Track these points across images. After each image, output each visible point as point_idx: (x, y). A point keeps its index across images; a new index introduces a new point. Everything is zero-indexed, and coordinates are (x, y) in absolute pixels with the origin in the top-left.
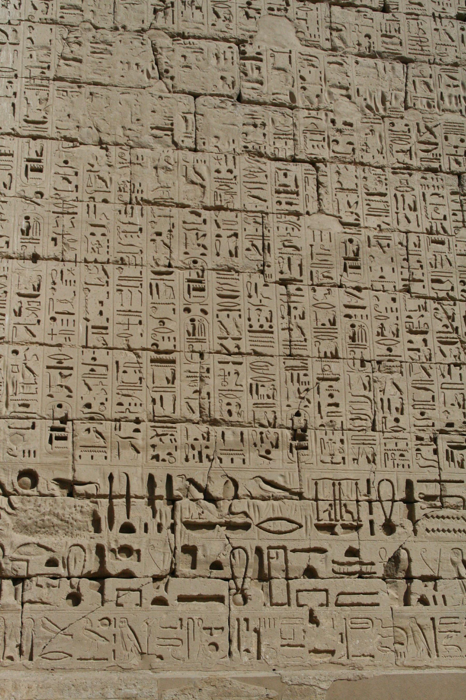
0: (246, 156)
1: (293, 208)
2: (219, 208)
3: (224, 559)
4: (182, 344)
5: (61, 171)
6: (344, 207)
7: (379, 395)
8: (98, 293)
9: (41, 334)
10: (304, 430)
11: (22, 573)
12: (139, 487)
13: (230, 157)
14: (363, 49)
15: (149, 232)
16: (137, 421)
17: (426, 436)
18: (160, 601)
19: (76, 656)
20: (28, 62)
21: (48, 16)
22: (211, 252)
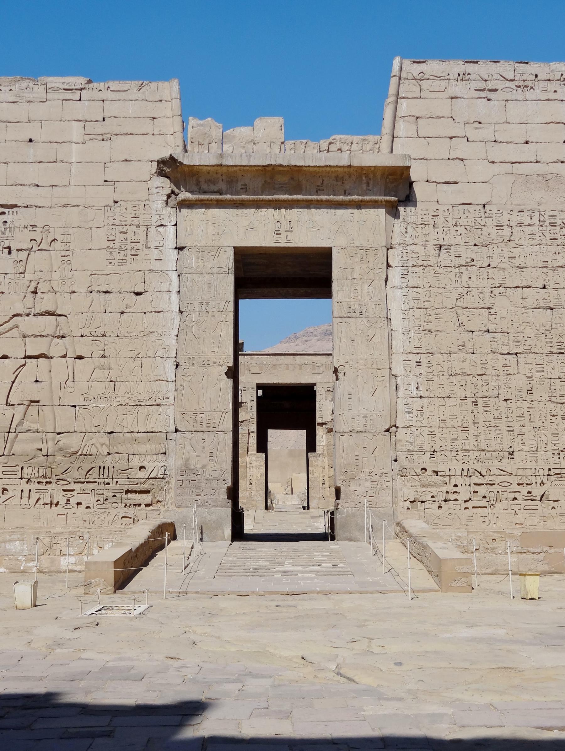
0: (492, 354)
1: (508, 373)
2: (482, 375)
3: (487, 495)
4: (471, 424)
5: (428, 365)
6: (527, 370)
7: (539, 439)
8: (442, 408)
9: (425, 423)
10: (513, 452)
11: (424, 500)
12: (459, 472)
13: (486, 355)
14: (535, 306)
15: (459, 385)
16: (457, 451)
17: (556, 453)
18: (466, 508)
19: (442, 525)
20: (413, 325)
21: (419, 306)
22: (480, 391)
